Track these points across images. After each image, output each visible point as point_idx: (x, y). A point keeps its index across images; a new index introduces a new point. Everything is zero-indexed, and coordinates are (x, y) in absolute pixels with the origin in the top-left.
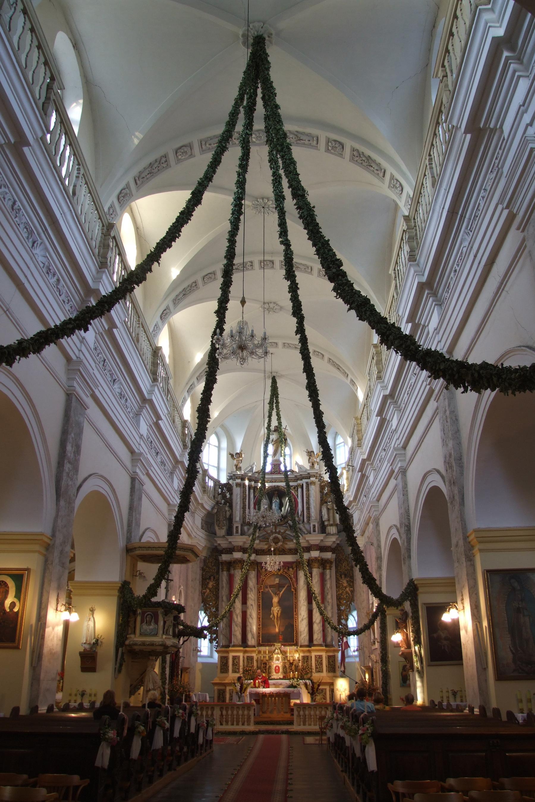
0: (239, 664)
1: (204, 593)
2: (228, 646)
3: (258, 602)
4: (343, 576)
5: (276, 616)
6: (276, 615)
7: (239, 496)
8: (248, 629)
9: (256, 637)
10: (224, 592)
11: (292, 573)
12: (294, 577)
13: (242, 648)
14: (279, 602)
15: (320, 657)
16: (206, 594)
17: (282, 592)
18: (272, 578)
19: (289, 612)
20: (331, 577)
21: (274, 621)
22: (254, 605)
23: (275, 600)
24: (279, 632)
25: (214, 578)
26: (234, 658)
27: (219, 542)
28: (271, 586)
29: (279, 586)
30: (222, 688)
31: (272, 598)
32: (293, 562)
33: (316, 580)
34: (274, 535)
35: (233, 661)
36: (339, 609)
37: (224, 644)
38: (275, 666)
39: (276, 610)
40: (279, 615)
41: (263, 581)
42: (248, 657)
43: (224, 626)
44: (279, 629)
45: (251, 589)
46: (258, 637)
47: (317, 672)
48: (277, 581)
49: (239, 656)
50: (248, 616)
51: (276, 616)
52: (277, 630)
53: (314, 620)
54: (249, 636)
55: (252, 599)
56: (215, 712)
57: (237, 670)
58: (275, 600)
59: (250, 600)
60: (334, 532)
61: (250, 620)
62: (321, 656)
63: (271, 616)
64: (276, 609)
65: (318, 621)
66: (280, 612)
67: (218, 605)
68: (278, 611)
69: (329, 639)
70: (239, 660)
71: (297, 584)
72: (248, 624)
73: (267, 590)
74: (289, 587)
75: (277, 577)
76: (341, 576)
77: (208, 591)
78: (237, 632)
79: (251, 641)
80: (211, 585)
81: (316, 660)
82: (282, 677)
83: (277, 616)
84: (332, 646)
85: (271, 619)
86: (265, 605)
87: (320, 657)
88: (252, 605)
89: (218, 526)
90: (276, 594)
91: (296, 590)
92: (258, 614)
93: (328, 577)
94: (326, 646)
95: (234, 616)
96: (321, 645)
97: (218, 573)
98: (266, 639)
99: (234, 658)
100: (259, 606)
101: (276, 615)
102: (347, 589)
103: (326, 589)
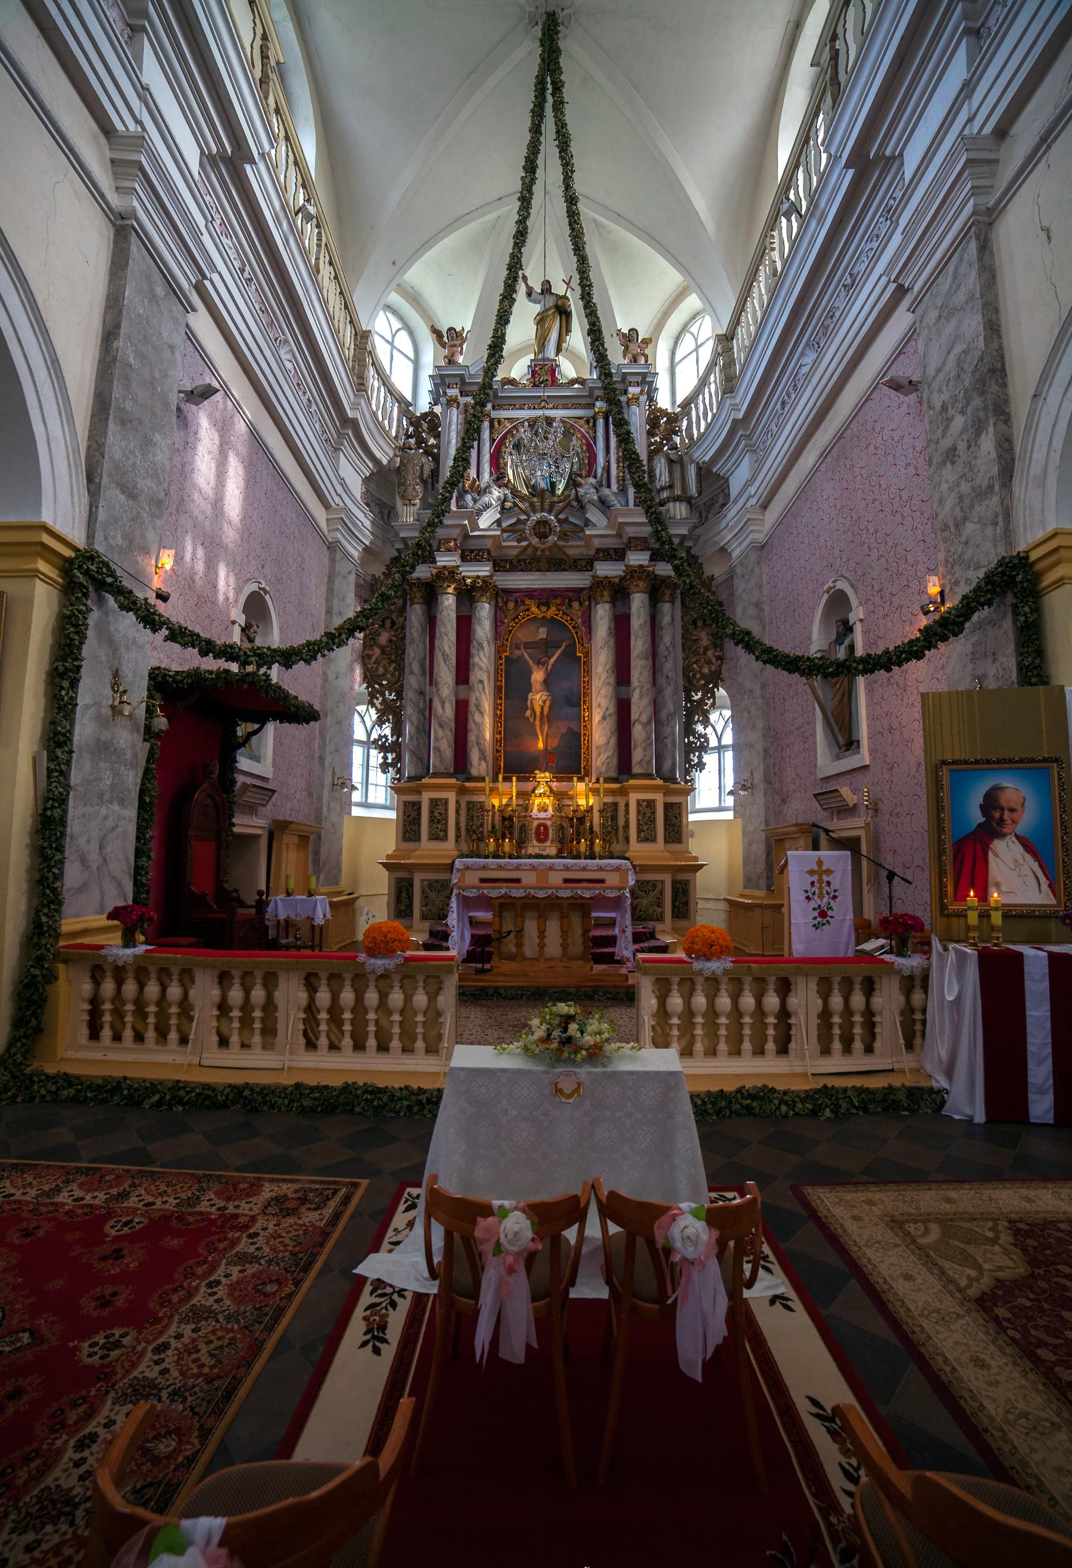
0: (446, 819)
1: (369, 657)
2: (420, 778)
3: (496, 680)
4: (699, 623)
5: (538, 714)
6: (538, 710)
7: (454, 427)
8: (472, 737)
9: (490, 758)
10: (413, 653)
11: (580, 613)
12: (583, 623)
13: (453, 781)
14: (546, 682)
15: (651, 804)
16: (374, 658)
17: (553, 660)
18: (532, 628)
19: (571, 701)
20: (673, 620)
21: (533, 724)
22: (486, 682)
23: (538, 676)
24: (546, 749)
25: (393, 623)
26: (434, 803)
27: (402, 535)
28: (527, 645)
29: (547, 646)
30: (403, 875)
31: (530, 674)
32: (581, 590)
33: (642, 621)
34: (538, 515)
35: (432, 812)
36: (688, 699)
37: (413, 774)
38: (536, 823)
39: (538, 698)
40: (546, 710)
41: (510, 631)
42: (469, 803)
43: (413, 729)
44: (546, 743)
45: (479, 644)
46: (496, 759)
47: (640, 840)
48: (542, 633)
49: (446, 801)
50: (472, 708)
51: (538, 714)
52: (541, 745)
53: (634, 716)
54: (474, 755)
55: (481, 669)
56: (279, 995)
57: (442, 834)
58: (538, 676)
59: (476, 669)
60: (684, 516)
61: (477, 717)
62: (654, 801)
63: (528, 713)
64: (538, 697)
65: (644, 718)
66: (548, 704)
67: (402, 686)
68: (544, 702)
69: (667, 766)
70: (446, 810)
71: (590, 640)
72: (471, 725)
73: (517, 652)
74: (572, 648)
75: (542, 626)
76: (694, 623)
77: (377, 651)
78: (442, 740)
79: (478, 766)
80: (384, 638)
81: (639, 812)
82: (553, 851)
83: (542, 713)
84: (673, 780)
85: (528, 718)
86: (512, 686)
87: (651, 804)
88: (481, 682)
89: (403, 497)
90: (538, 663)
91: (588, 654)
92: (496, 707)
93: (666, 620)
94: (665, 780)
95: (437, 704)
96: (649, 776)
97: (402, 610)
98: (516, 766)
99: (434, 803)
100: (498, 689)
101: (538, 710)
102: (710, 653)
103: (662, 647)
